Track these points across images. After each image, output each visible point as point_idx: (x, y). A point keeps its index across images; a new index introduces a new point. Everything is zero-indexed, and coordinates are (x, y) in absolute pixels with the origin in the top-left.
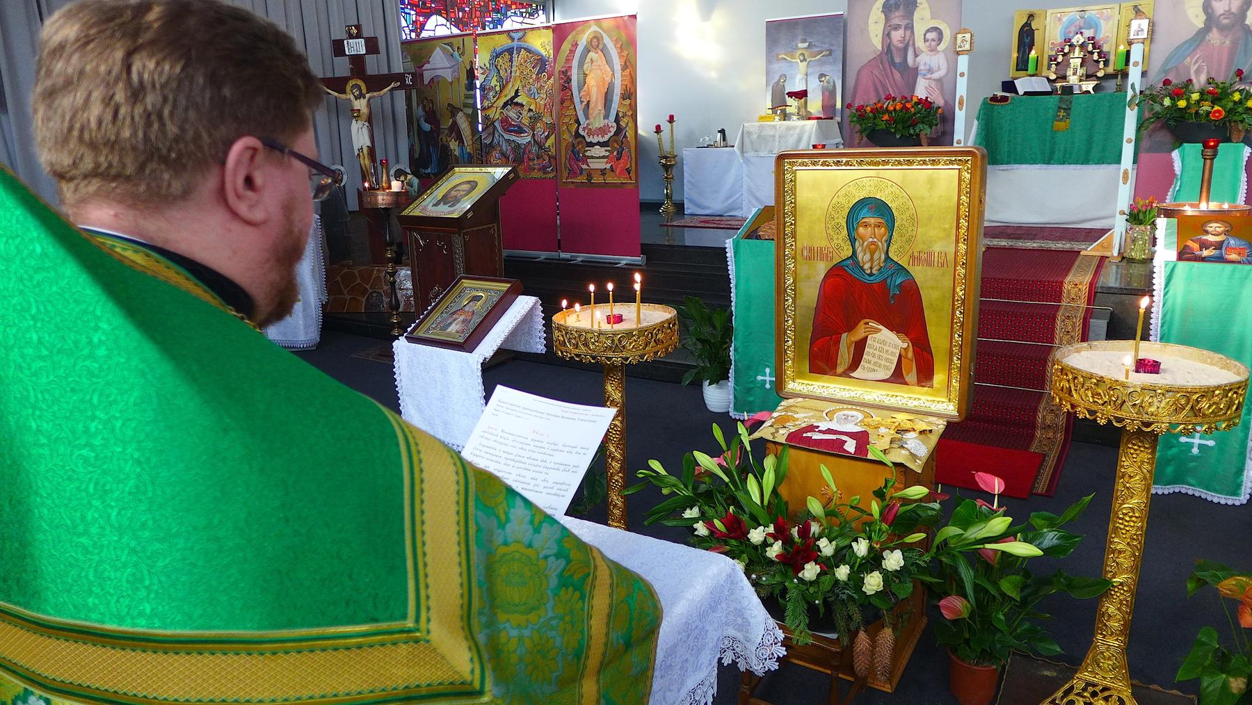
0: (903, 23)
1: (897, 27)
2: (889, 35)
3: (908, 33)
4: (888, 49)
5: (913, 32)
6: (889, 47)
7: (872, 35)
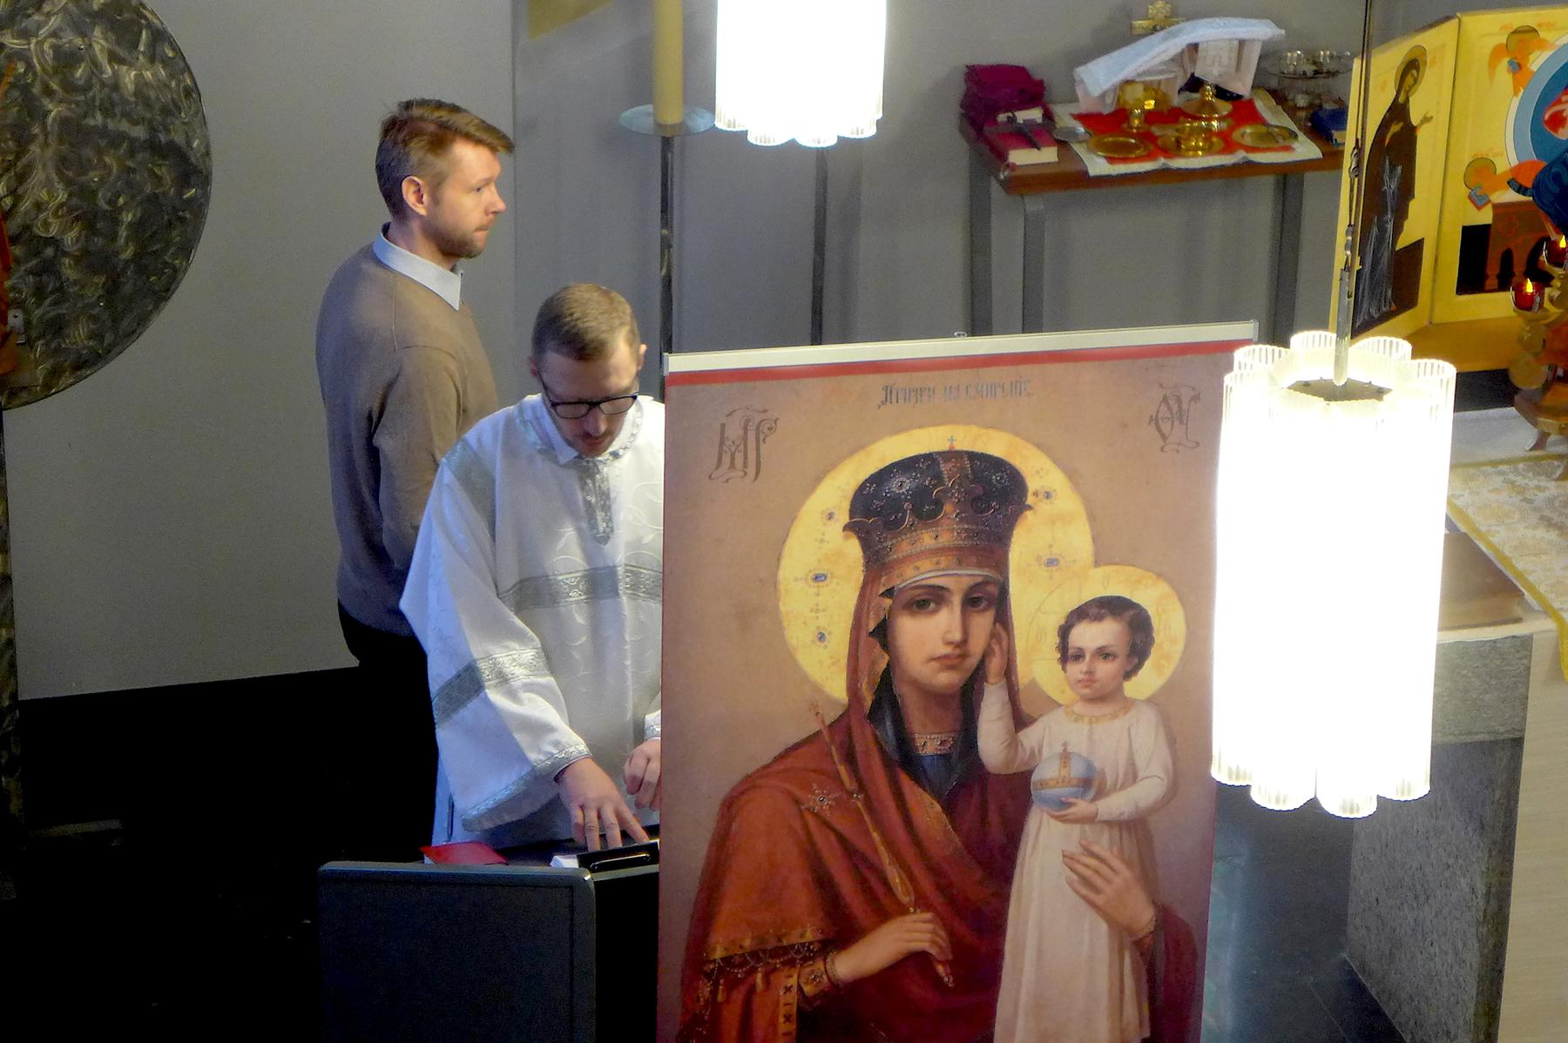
0: (958, 580)
1: (927, 600)
2: (884, 633)
3: (983, 623)
5: (1003, 618)
6: (886, 685)
7: (798, 635)
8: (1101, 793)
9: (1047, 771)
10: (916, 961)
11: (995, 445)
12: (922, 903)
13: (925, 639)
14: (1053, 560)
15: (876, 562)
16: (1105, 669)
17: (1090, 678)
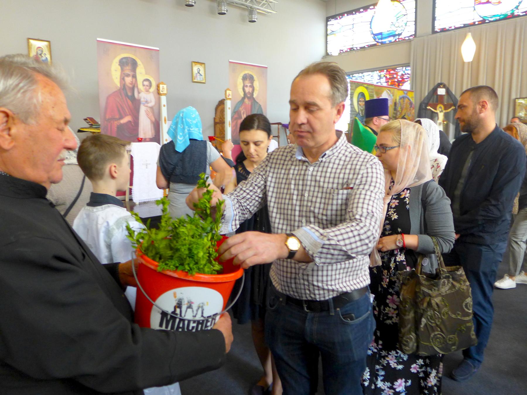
1: (128, 75)
4: (124, 86)
5: (136, 80)
8: (148, 103)
9: (142, 100)
10: (129, 122)
11: (134, 57)
12: (130, 115)
13: (128, 80)
14: (141, 74)
15: (122, 70)
16: (148, 88)
17: (146, 89)
